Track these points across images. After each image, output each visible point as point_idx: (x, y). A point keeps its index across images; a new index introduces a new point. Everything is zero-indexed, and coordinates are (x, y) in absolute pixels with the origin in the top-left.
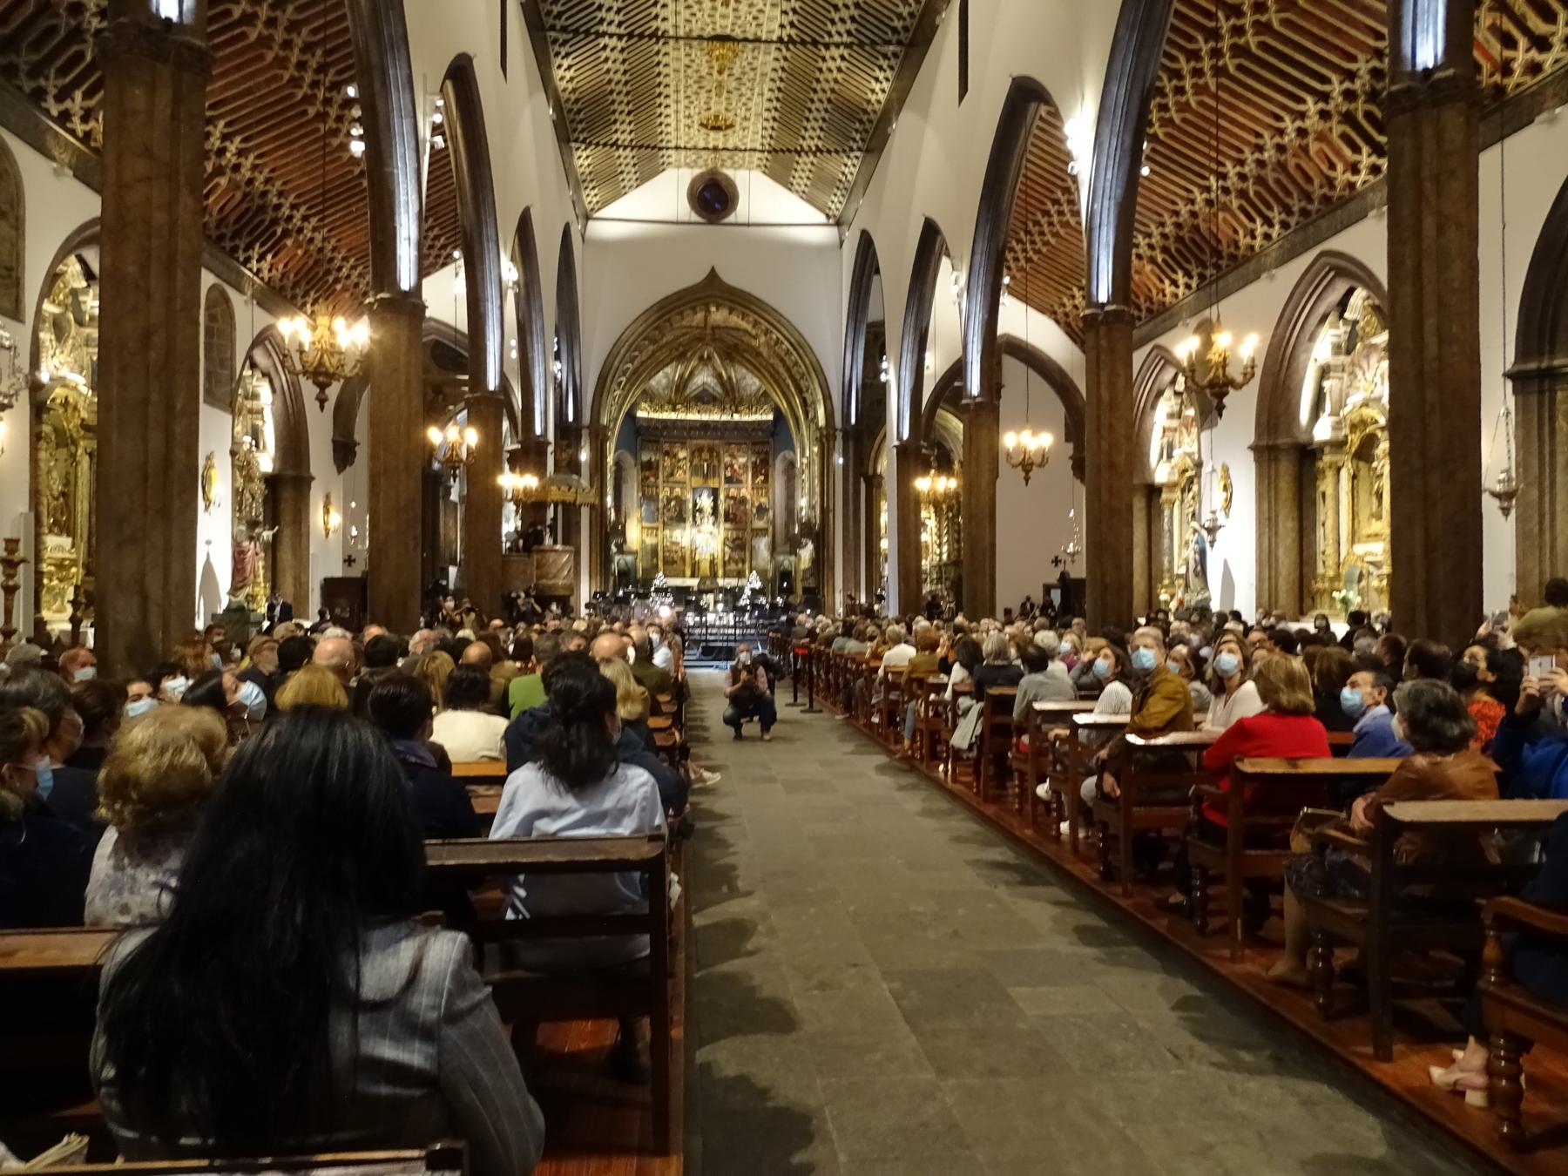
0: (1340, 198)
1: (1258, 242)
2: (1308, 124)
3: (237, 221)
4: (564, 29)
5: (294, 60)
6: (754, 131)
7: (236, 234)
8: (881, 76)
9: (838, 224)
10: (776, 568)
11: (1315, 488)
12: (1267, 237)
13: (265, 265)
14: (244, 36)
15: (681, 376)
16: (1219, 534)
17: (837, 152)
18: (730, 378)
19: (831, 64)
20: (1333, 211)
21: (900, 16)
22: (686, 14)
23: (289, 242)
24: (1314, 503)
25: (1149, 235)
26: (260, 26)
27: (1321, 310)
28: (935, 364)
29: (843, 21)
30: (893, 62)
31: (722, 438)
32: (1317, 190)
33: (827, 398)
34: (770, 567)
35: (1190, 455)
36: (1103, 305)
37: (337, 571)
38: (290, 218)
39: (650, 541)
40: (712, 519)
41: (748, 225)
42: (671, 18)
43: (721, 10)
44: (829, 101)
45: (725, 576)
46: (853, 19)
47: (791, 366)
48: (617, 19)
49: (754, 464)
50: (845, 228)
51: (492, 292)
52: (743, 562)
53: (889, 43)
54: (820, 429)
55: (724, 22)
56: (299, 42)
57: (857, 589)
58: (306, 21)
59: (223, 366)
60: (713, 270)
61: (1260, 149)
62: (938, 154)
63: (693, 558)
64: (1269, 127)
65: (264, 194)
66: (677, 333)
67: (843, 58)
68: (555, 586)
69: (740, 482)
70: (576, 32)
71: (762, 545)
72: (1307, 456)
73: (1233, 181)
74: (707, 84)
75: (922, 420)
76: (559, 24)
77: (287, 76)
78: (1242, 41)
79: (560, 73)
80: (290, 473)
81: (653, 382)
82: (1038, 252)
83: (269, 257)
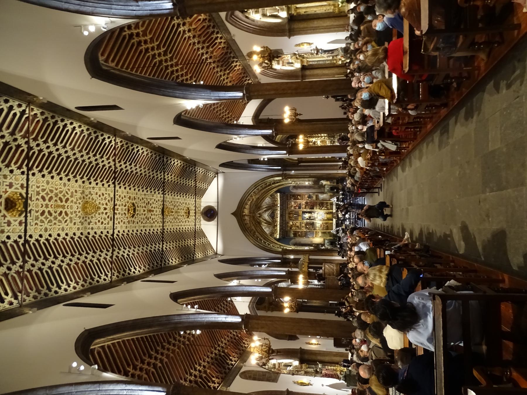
0: (209, 16)
1: (223, 41)
2: (187, 29)
3: (220, 367)
4: (161, 262)
5: (173, 348)
6: (189, 201)
7: (224, 368)
8: (173, 162)
9: (217, 174)
10: (329, 192)
11: (303, 15)
12: (221, 38)
13: (233, 359)
14: (166, 363)
15: (265, 223)
16: (319, 48)
17: (195, 175)
18: (266, 207)
19: (170, 178)
20: (213, 18)
21: (156, 157)
22: (156, 223)
23: (226, 351)
24: (308, 15)
25: (221, 76)
26: (163, 358)
27: (244, 19)
28: (262, 143)
29: (157, 175)
30: (169, 159)
31: (285, 210)
32: (206, 24)
33: (272, 176)
34: (329, 194)
35: (291, 57)
36: (244, 94)
37: (331, 342)
38: (219, 350)
39: (320, 234)
40: (313, 214)
42: (157, 227)
43: (155, 212)
44: (180, 178)
45: (332, 209)
46: (156, 172)
47: (262, 188)
48: (158, 245)
49: (294, 199)
50: (219, 172)
51: (241, 289)
52: (327, 203)
53: (163, 160)
54: (283, 179)
55: (158, 211)
56: (167, 346)
57: (337, 165)
58: (161, 343)
59: (265, 375)
60: (232, 214)
61: (194, 43)
62: (197, 145)
63: (326, 220)
64: (188, 41)
65: (212, 358)
66: (252, 225)
67: (168, 174)
68: (336, 270)
69: (300, 204)
70: (162, 258)
71: (321, 196)
72: (292, 19)
73: (204, 51)
75: (280, 146)
76: (160, 263)
77: (178, 350)
78: (162, 53)
79: (174, 262)
80: (299, 355)
81: (268, 233)
82: (226, 111)
83: (231, 358)
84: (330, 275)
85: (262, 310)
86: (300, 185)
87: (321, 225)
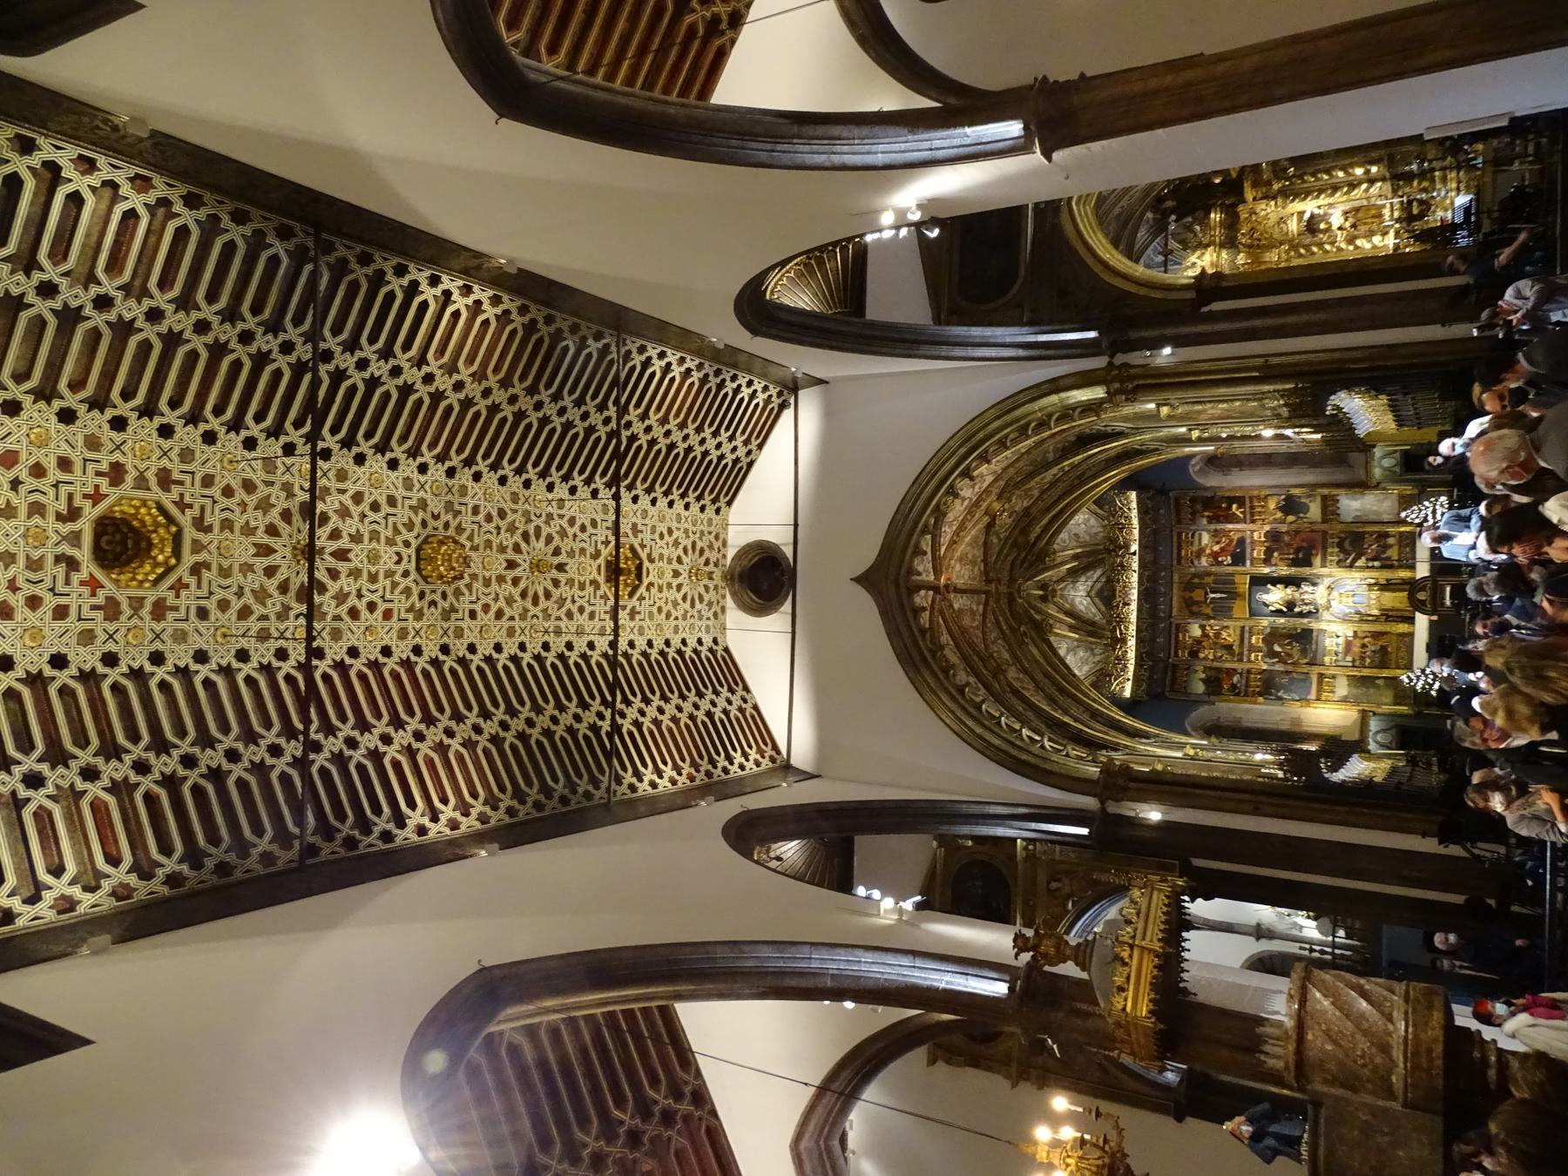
9: (792, 387)
10: (1393, 477)
15: (1072, 628)
18: (1075, 557)
31: (1170, 569)
33: (1055, 385)
34: (1395, 490)
39: (1342, 688)
40: (1305, 588)
41: (796, 525)
45: (1412, 567)
63: (1377, 619)
68: (1414, 1050)
69: (1241, 541)
71: (1353, 505)
74: (540, 584)
85: (989, 1069)
87: (1348, 645)
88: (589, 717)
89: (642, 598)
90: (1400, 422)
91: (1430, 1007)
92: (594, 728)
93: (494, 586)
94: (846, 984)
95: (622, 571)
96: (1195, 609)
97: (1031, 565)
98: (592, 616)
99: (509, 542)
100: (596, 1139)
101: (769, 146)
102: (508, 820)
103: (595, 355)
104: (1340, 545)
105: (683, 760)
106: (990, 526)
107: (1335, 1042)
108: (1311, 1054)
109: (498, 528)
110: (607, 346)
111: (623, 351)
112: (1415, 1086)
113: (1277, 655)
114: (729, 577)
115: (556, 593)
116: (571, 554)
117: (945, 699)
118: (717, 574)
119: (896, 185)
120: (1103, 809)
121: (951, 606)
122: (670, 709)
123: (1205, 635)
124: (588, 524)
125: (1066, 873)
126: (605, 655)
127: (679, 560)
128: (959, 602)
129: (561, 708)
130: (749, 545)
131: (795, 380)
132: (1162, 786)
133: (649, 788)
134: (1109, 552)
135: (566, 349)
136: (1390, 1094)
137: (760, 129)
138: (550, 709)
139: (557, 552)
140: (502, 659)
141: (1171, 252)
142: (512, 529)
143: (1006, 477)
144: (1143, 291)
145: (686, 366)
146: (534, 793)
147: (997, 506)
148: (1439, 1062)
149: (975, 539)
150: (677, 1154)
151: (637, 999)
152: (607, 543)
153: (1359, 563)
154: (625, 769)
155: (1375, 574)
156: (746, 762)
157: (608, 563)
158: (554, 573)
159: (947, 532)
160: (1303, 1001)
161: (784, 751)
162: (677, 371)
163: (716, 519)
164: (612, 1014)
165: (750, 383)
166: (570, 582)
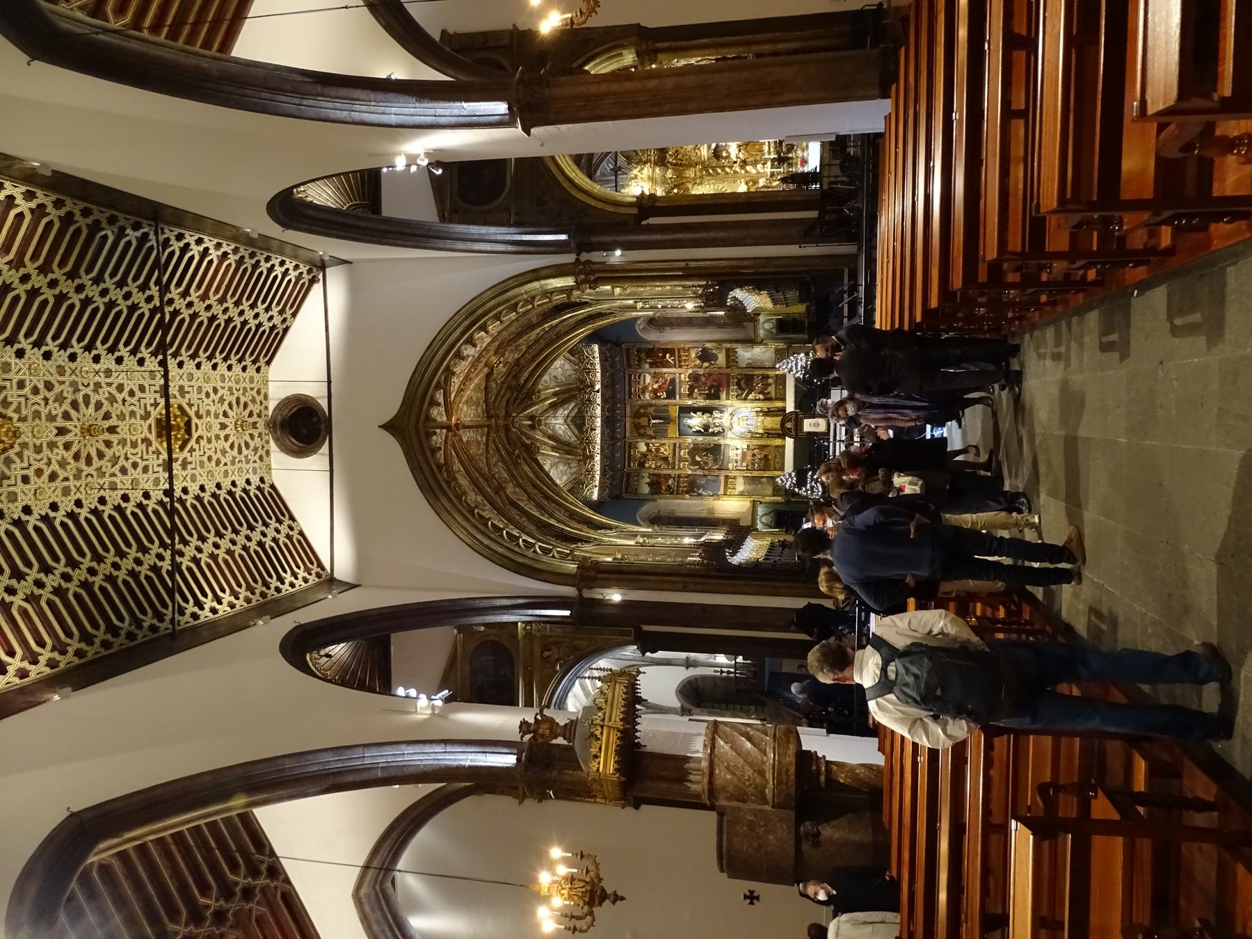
9: (322, 266)
10: (772, 337)
15: (554, 449)
18: (555, 394)
33: (536, 275)
34: (773, 346)
39: (740, 486)
40: (716, 414)
41: (329, 382)
45: (784, 399)
49: (652, 365)
52: (767, 377)
54: (579, 285)
60: (389, 427)
68: (779, 771)
69: (673, 381)
71: (746, 354)
84: (742, 797)
85: (503, 793)
86: (671, 313)
87: (744, 454)
88: (149, 560)
89: (192, 450)
90: (775, 302)
91: (788, 742)
92: (155, 569)
93: (46, 452)
94: (393, 773)
95: (172, 428)
96: (642, 431)
97: (523, 401)
98: (145, 470)
99: (58, 410)
100: (186, 925)
101: (297, 101)
102: (76, 661)
103: (134, 243)
104: (738, 384)
105: (240, 586)
106: (488, 376)
107: (733, 773)
108: (718, 782)
109: (46, 400)
110: (146, 235)
111: (161, 238)
112: (779, 794)
113: (697, 463)
114: (272, 425)
115: (109, 453)
116: (121, 417)
117: (459, 519)
118: (261, 424)
119: (406, 139)
120: (581, 595)
121: (461, 440)
122: (225, 544)
123: (649, 450)
124: (136, 389)
125: (555, 643)
126: (161, 503)
127: (225, 414)
128: (466, 436)
129: (121, 554)
130: (287, 398)
131: (323, 261)
132: (621, 574)
133: (210, 615)
134: (580, 390)
135: (105, 238)
136: (764, 800)
137: (288, 87)
138: (111, 557)
139: (107, 416)
140: (59, 517)
141: (620, 168)
142: (60, 399)
143: (500, 339)
144: (600, 205)
145: (223, 250)
146: (101, 635)
147: (494, 359)
148: (793, 777)
149: (478, 386)
150: (257, 921)
151: (217, 813)
152: (156, 405)
153: (750, 397)
154: (187, 601)
155: (760, 404)
156: (296, 581)
157: (158, 421)
158: (107, 436)
159: (456, 382)
160: (713, 747)
161: (327, 566)
162: (214, 255)
163: (257, 377)
164: (198, 828)
165: (282, 263)
166: (123, 442)
